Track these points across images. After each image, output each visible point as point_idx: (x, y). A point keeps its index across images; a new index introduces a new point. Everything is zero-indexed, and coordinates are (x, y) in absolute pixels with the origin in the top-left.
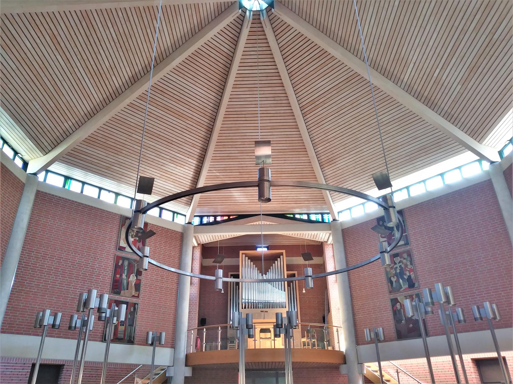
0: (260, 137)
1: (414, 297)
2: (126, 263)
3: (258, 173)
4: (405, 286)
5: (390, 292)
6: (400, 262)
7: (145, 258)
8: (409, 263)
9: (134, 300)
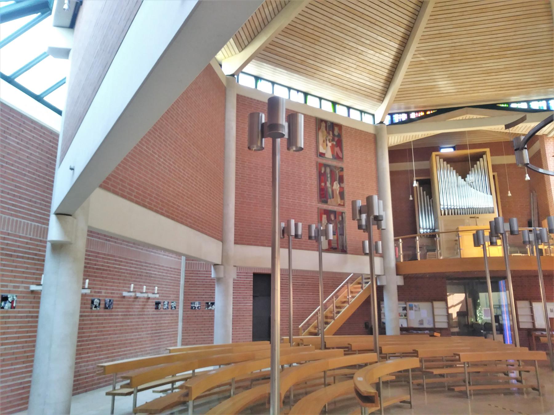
9: (340, 209)
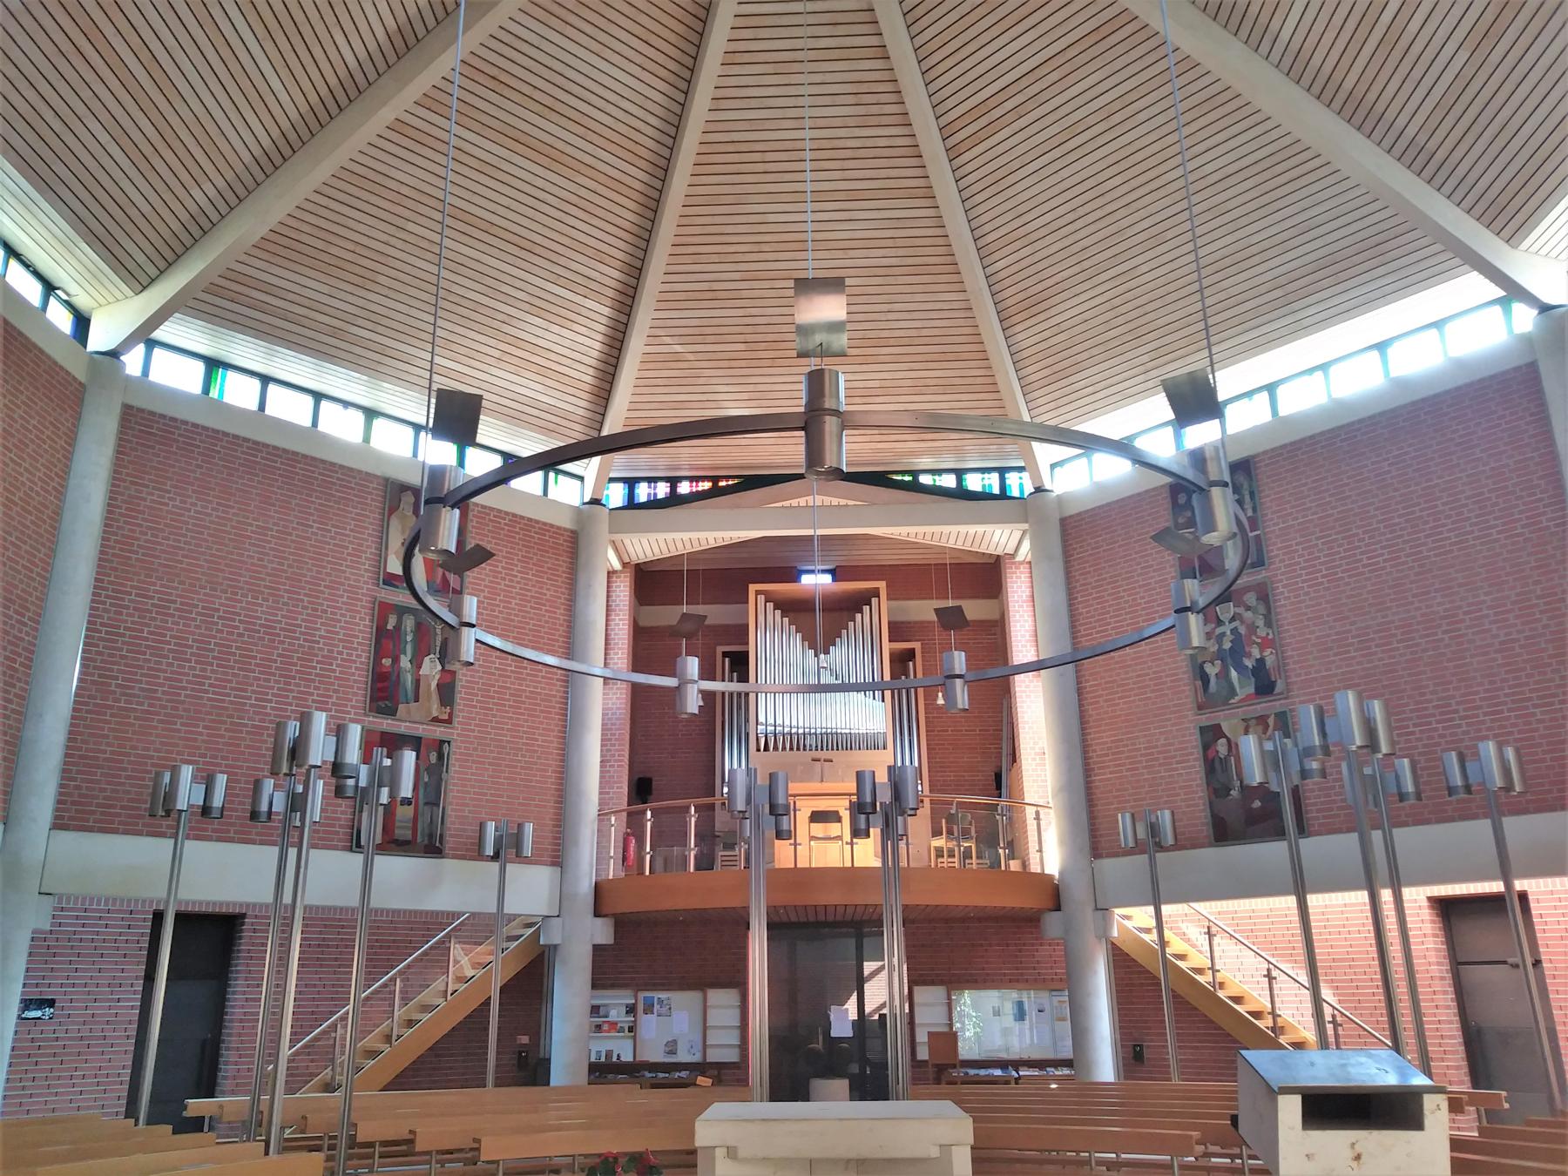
0: (811, 264)
1: (1271, 721)
2: (409, 623)
3: (803, 387)
4: (1243, 687)
5: (1200, 707)
6: (1233, 619)
7: (465, 630)
8: (1260, 622)
9: (439, 732)
